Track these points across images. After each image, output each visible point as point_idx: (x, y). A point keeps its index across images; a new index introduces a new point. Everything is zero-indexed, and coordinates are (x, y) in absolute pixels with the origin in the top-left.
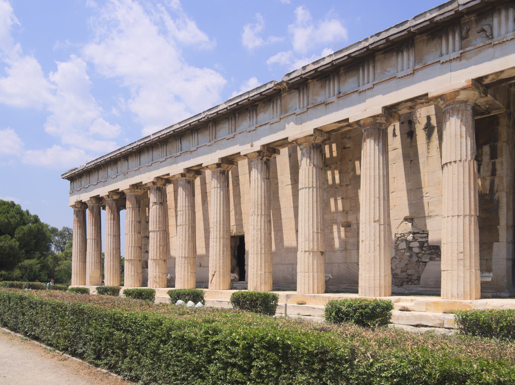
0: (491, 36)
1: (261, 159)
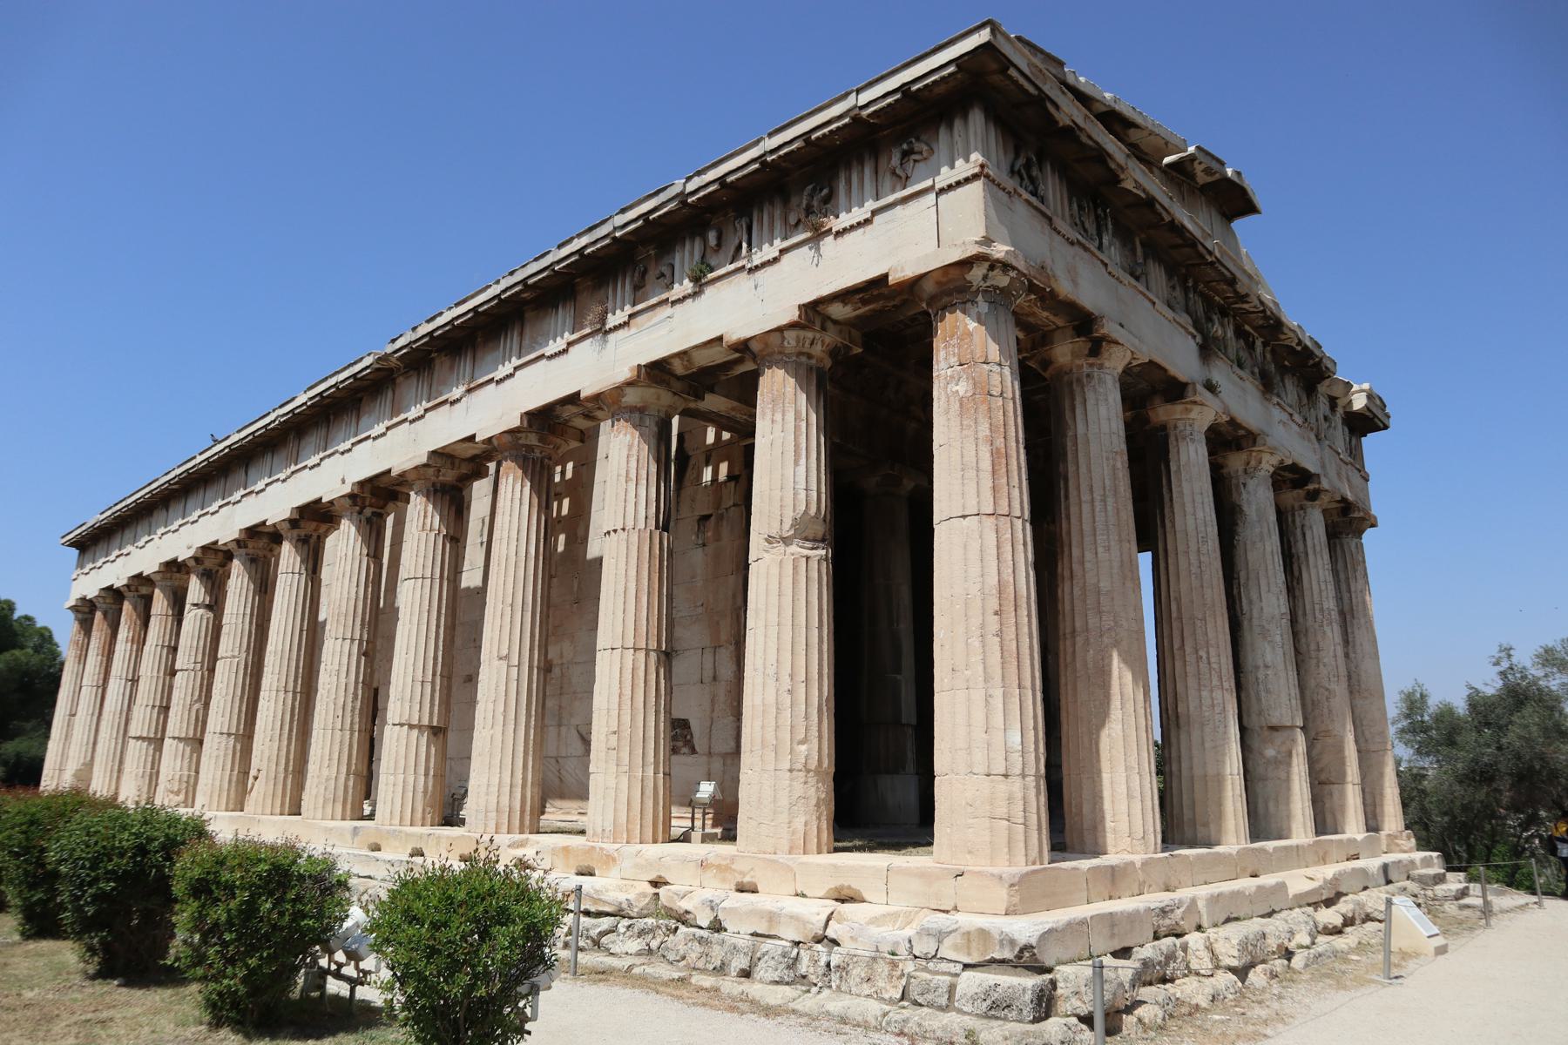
1: (360, 513)
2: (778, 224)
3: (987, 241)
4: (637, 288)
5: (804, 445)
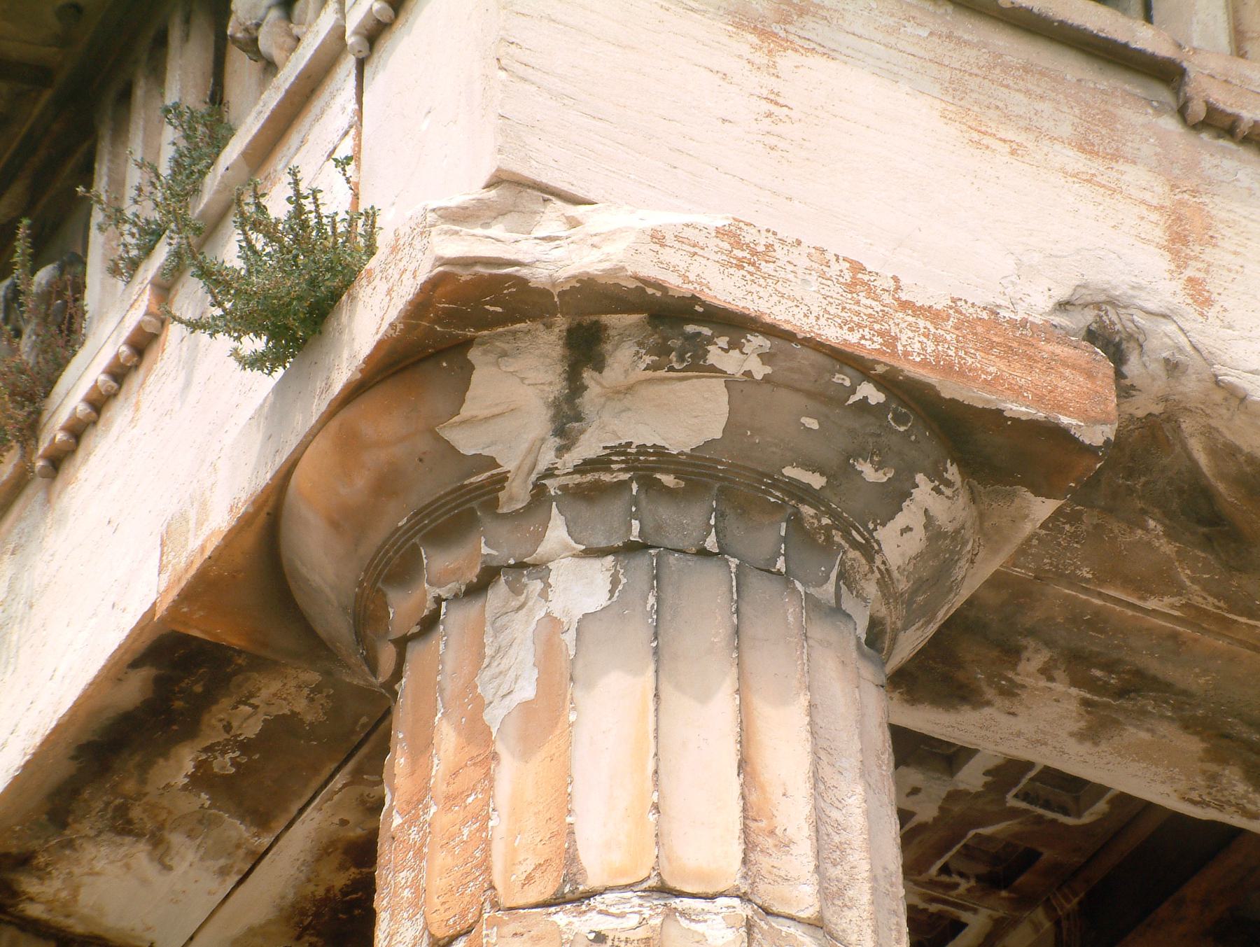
3: (516, 190)
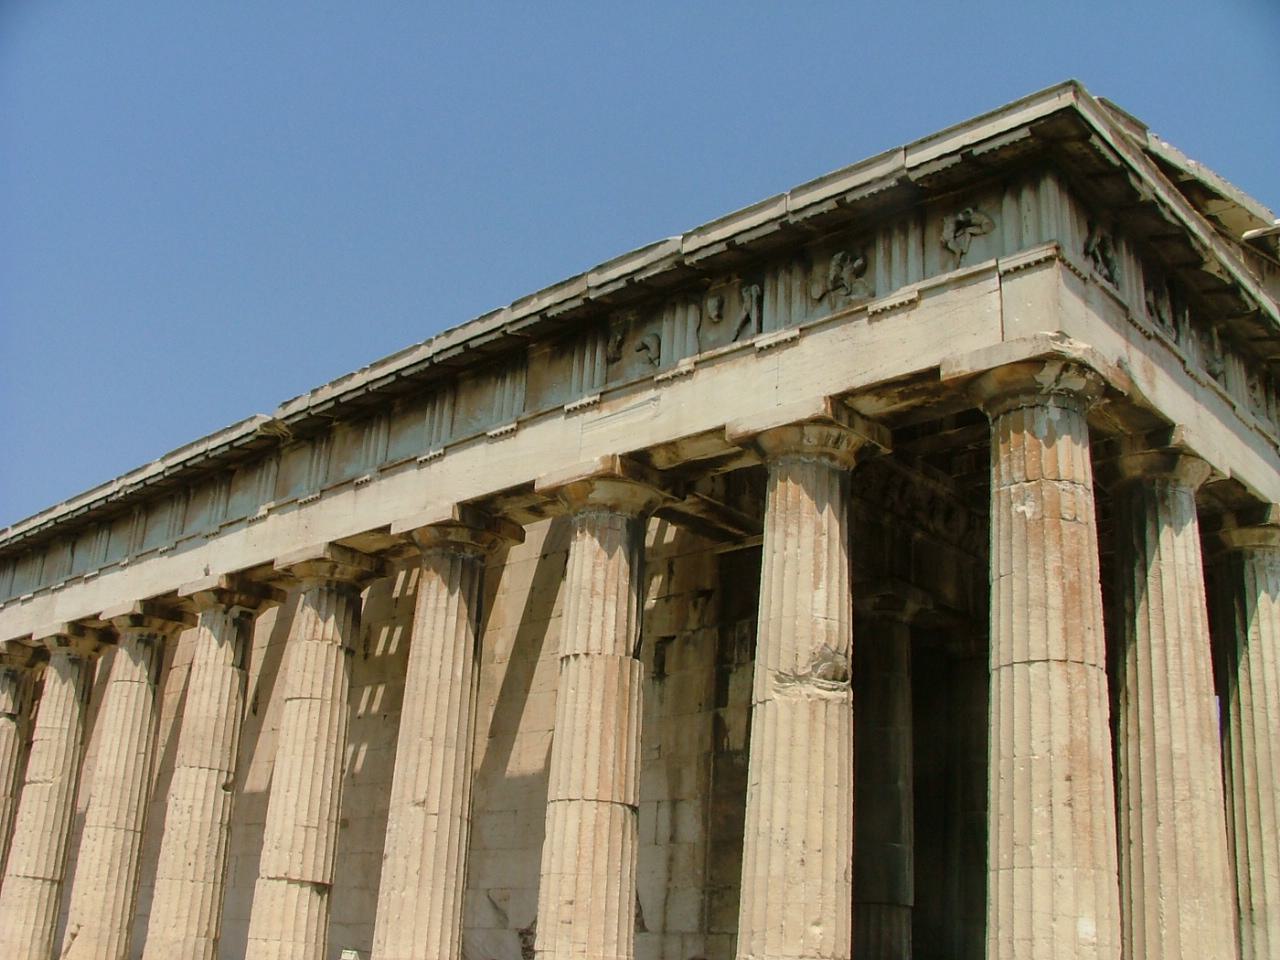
0: (654, 362)
1: (226, 612)
2: (797, 297)
3: (1062, 336)
4: (610, 361)
5: (824, 565)
